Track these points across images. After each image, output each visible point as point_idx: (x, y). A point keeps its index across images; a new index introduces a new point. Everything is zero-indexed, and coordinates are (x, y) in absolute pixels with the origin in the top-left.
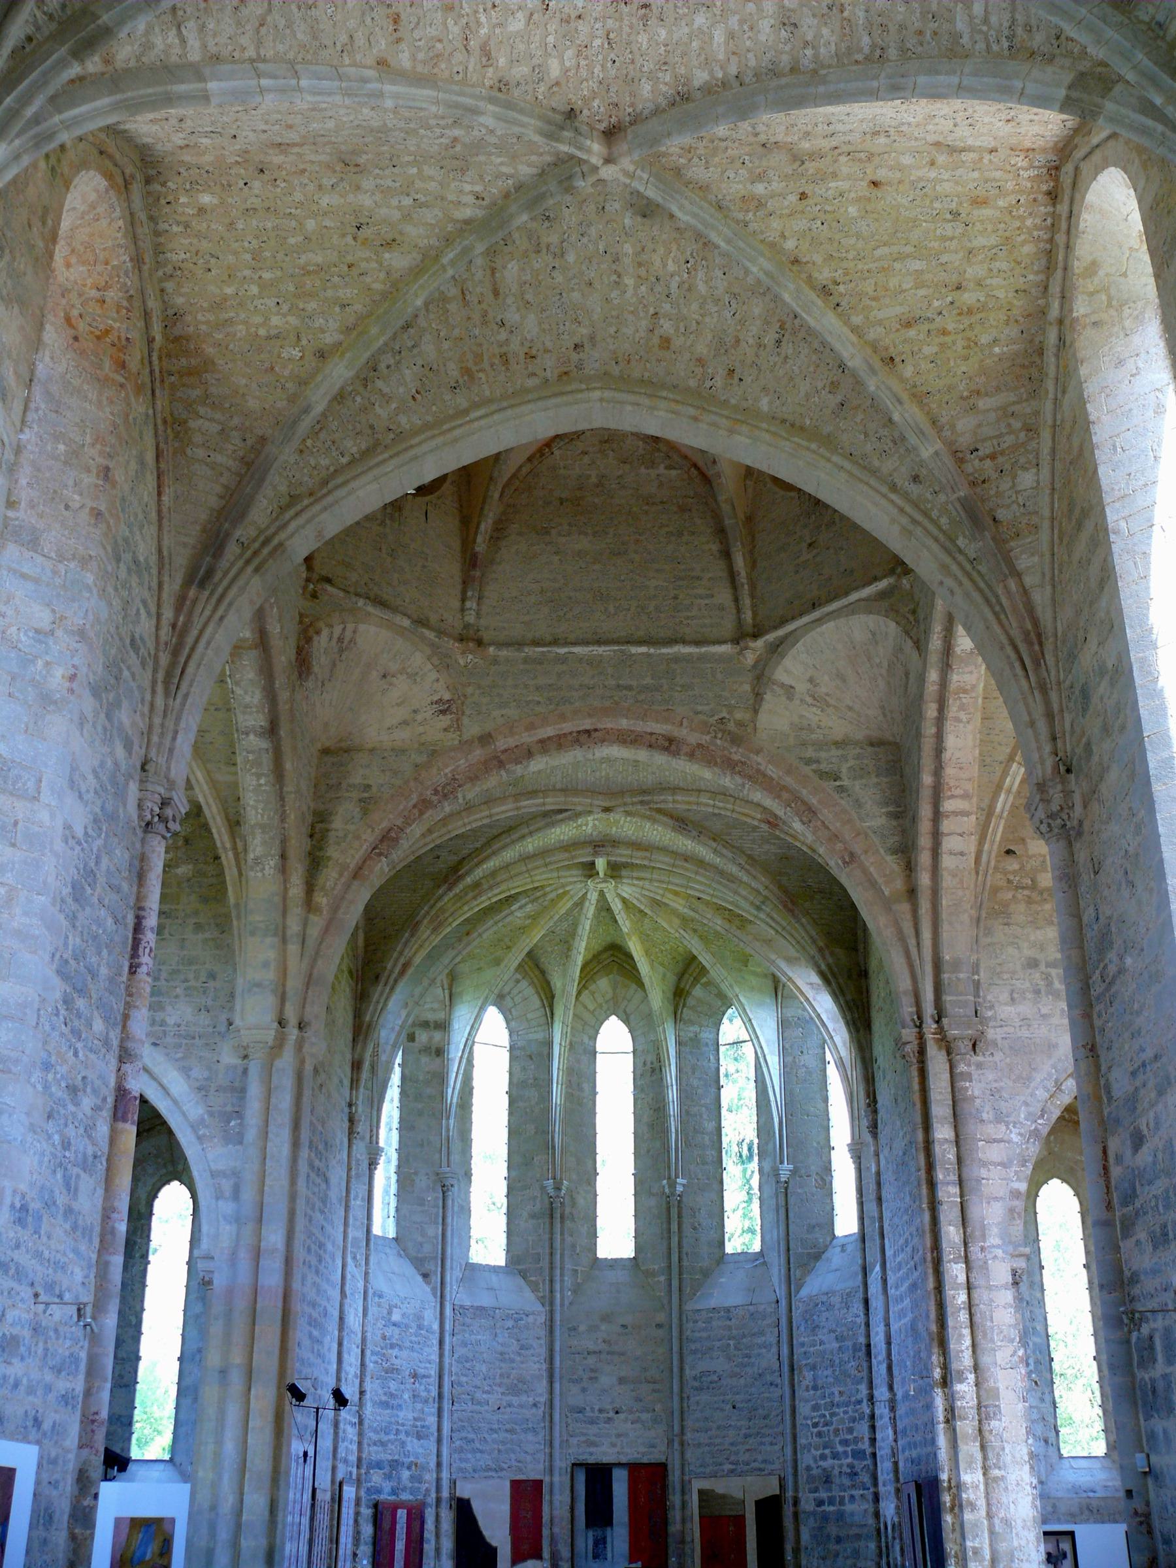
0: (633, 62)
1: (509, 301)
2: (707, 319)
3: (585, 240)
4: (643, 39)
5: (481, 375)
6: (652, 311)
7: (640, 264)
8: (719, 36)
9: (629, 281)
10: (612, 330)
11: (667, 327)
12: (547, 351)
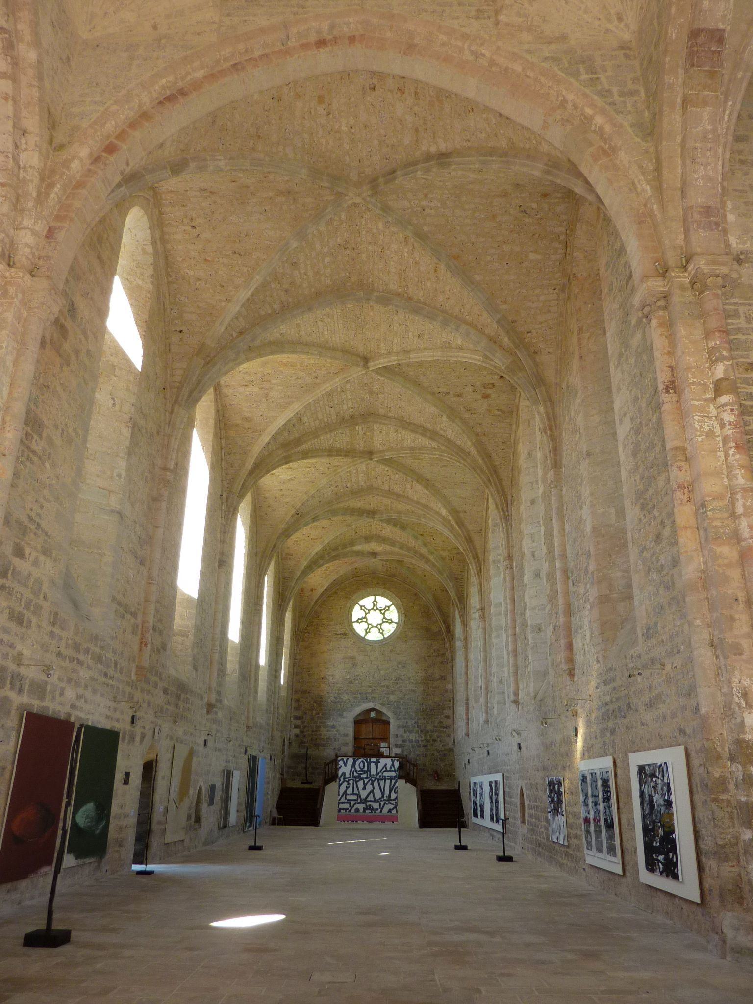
0: (349, 226)
1: (410, 125)
2: (300, 121)
3: (368, 150)
4: (346, 236)
5: (432, 94)
6: (331, 116)
7: (340, 139)
8: (318, 246)
9: (345, 129)
10: (353, 99)
11: (321, 110)
12: (391, 91)
